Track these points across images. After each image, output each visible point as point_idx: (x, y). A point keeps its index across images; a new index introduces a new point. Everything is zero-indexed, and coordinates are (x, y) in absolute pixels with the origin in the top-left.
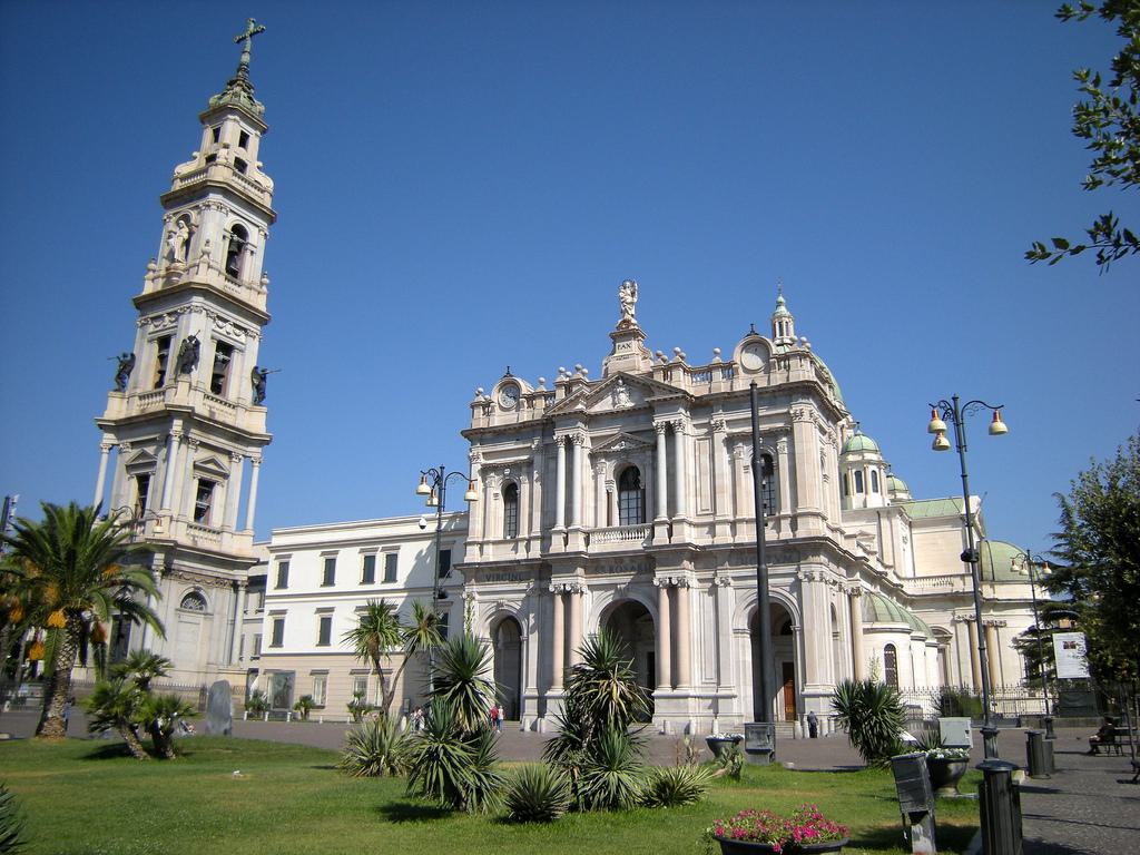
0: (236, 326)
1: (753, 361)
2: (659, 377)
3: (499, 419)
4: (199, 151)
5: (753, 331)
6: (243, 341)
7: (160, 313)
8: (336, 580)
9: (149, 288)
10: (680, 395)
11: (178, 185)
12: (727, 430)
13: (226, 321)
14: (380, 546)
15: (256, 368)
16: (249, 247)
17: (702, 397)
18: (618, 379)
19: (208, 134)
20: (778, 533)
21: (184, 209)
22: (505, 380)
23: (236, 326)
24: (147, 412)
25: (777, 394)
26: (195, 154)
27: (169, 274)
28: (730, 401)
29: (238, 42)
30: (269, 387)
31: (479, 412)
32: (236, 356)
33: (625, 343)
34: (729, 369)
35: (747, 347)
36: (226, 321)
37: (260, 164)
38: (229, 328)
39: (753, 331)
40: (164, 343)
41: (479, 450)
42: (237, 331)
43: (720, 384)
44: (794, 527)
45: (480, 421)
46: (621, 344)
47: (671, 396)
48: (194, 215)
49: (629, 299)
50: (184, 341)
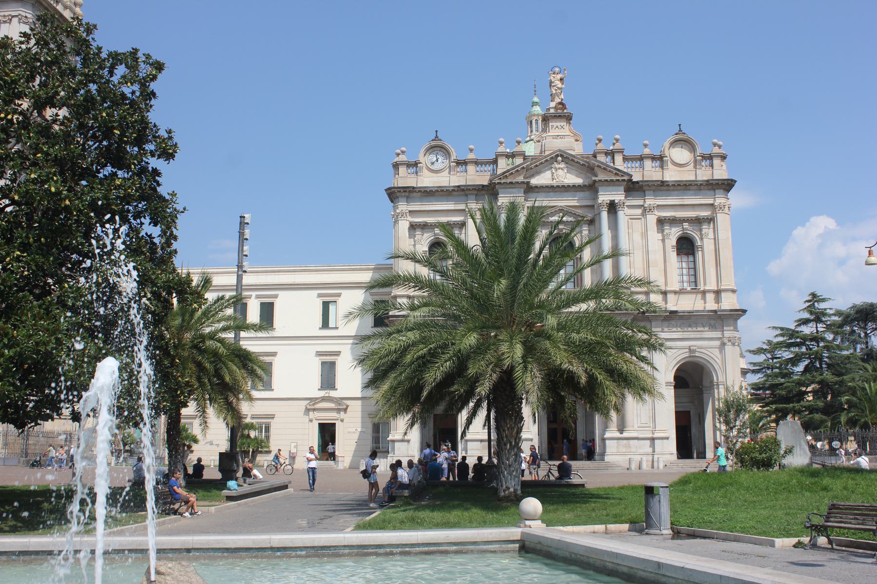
1: (681, 155)
2: (601, 158)
3: (427, 180)
5: (680, 130)
10: (626, 178)
12: (656, 212)
14: (254, 294)
17: (637, 182)
18: (557, 156)
20: (705, 303)
22: (433, 143)
25: (702, 187)
28: (662, 187)
31: (402, 170)
33: (558, 124)
34: (660, 159)
35: (675, 143)
39: (680, 130)
41: (403, 207)
43: (650, 172)
44: (718, 300)
45: (405, 178)
46: (555, 124)
47: (618, 178)
49: (560, 85)
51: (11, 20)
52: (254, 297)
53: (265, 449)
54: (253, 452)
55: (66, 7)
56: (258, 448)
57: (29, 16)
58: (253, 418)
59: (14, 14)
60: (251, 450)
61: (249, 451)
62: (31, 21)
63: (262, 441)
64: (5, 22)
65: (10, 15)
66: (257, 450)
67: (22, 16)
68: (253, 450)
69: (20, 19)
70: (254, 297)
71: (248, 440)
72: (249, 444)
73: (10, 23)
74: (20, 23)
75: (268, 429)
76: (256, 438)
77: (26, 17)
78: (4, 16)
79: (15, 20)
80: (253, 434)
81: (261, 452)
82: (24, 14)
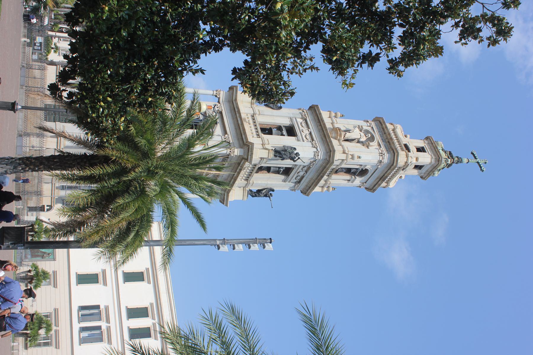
0: (303, 177)
4: (410, 138)
6: (292, 181)
7: (310, 126)
8: (128, 284)
9: (325, 115)
11: (390, 127)
13: (306, 172)
15: (273, 190)
16: (353, 177)
19: (421, 144)
21: (377, 136)
23: (303, 177)
24: (244, 123)
26: (408, 136)
27: (337, 130)
29: (472, 153)
30: (261, 200)
32: (283, 177)
36: (306, 172)
37: (403, 178)
38: (301, 174)
40: (291, 131)
42: (299, 178)
48: (374, 144)
50: (295, 149)
51: (314, 147)
52: (154, 321)
53: (28, 345)
54: (27, 334)
55: (326, 181)
56: (30, 337)
57: (319, 158)
58: (56, 331)
59: (318, 148)
60: (28, 332)
61: (27, 330)
62: (317, 158)
63: (36, 340)
64: (312, 144)
65: (317, 147)
66: (28, 337)
67: (318, 153)
68: (28, 334)
69: (316, 152)
70: (154, 321)
71: (37, 328)
72: (34, 328)
73: (312, 147)
74: (314, 152)
75: (46, 344)
76: (38, 335)
77: (318, 155)
78: (316, 144)
79: (315, 150)
80: (42, 332)
81: (26, 340)
82: (320, 154)
